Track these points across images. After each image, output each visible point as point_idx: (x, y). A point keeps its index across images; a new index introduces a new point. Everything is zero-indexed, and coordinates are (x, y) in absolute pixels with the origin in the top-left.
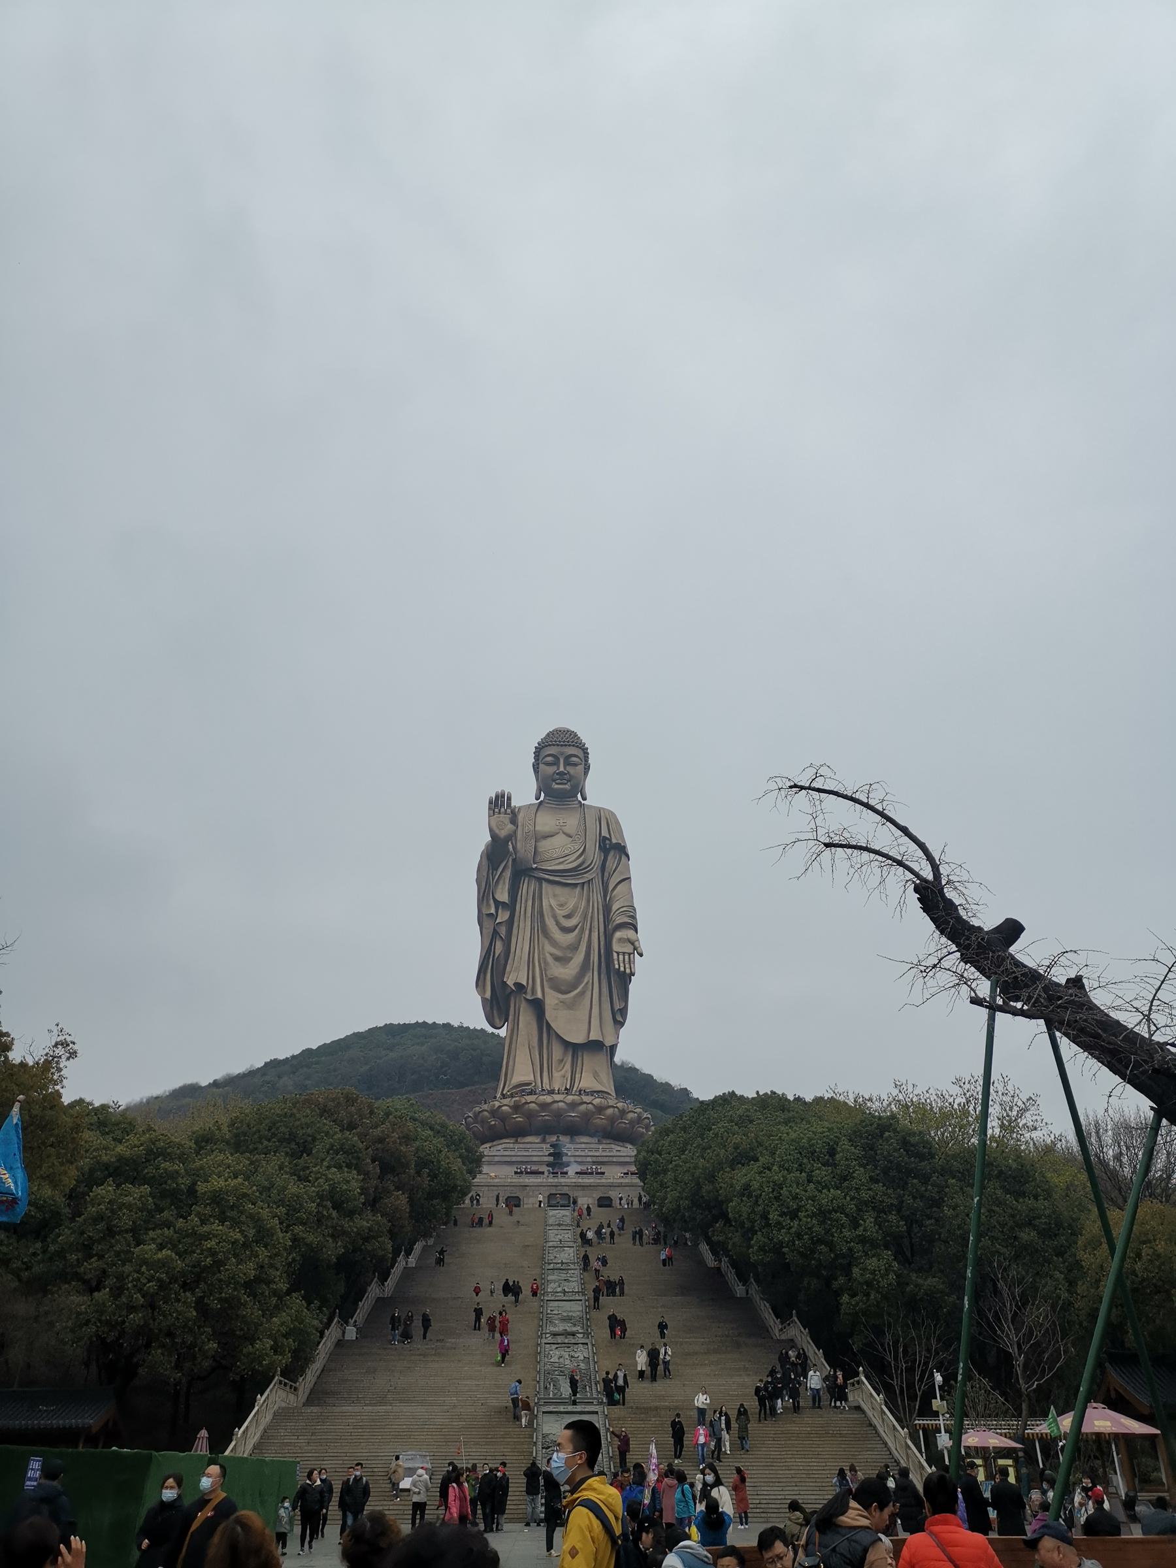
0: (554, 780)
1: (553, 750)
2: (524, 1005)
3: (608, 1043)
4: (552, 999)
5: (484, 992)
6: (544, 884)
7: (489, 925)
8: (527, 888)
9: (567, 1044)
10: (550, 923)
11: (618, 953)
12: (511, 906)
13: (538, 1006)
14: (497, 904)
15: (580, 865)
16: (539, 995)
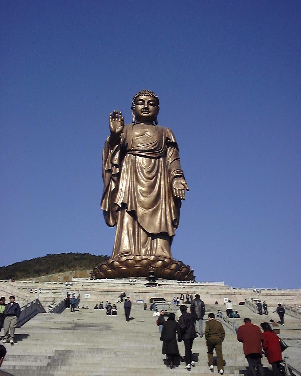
0: (142, 112)
1: (143, 98)
2: (126, 213)
3: (171, 234)
4: (140, 211)
5: (105, 207)
6: (137, 157)
7: (108, 175)
8: (128, 158)
9: (149, 235)
10: (140, 175)
11: (176, 189)
12: (120, 166)
13: (133, 214)
14: (113, 165)
15: (155, 149)
16: (134, 209)
